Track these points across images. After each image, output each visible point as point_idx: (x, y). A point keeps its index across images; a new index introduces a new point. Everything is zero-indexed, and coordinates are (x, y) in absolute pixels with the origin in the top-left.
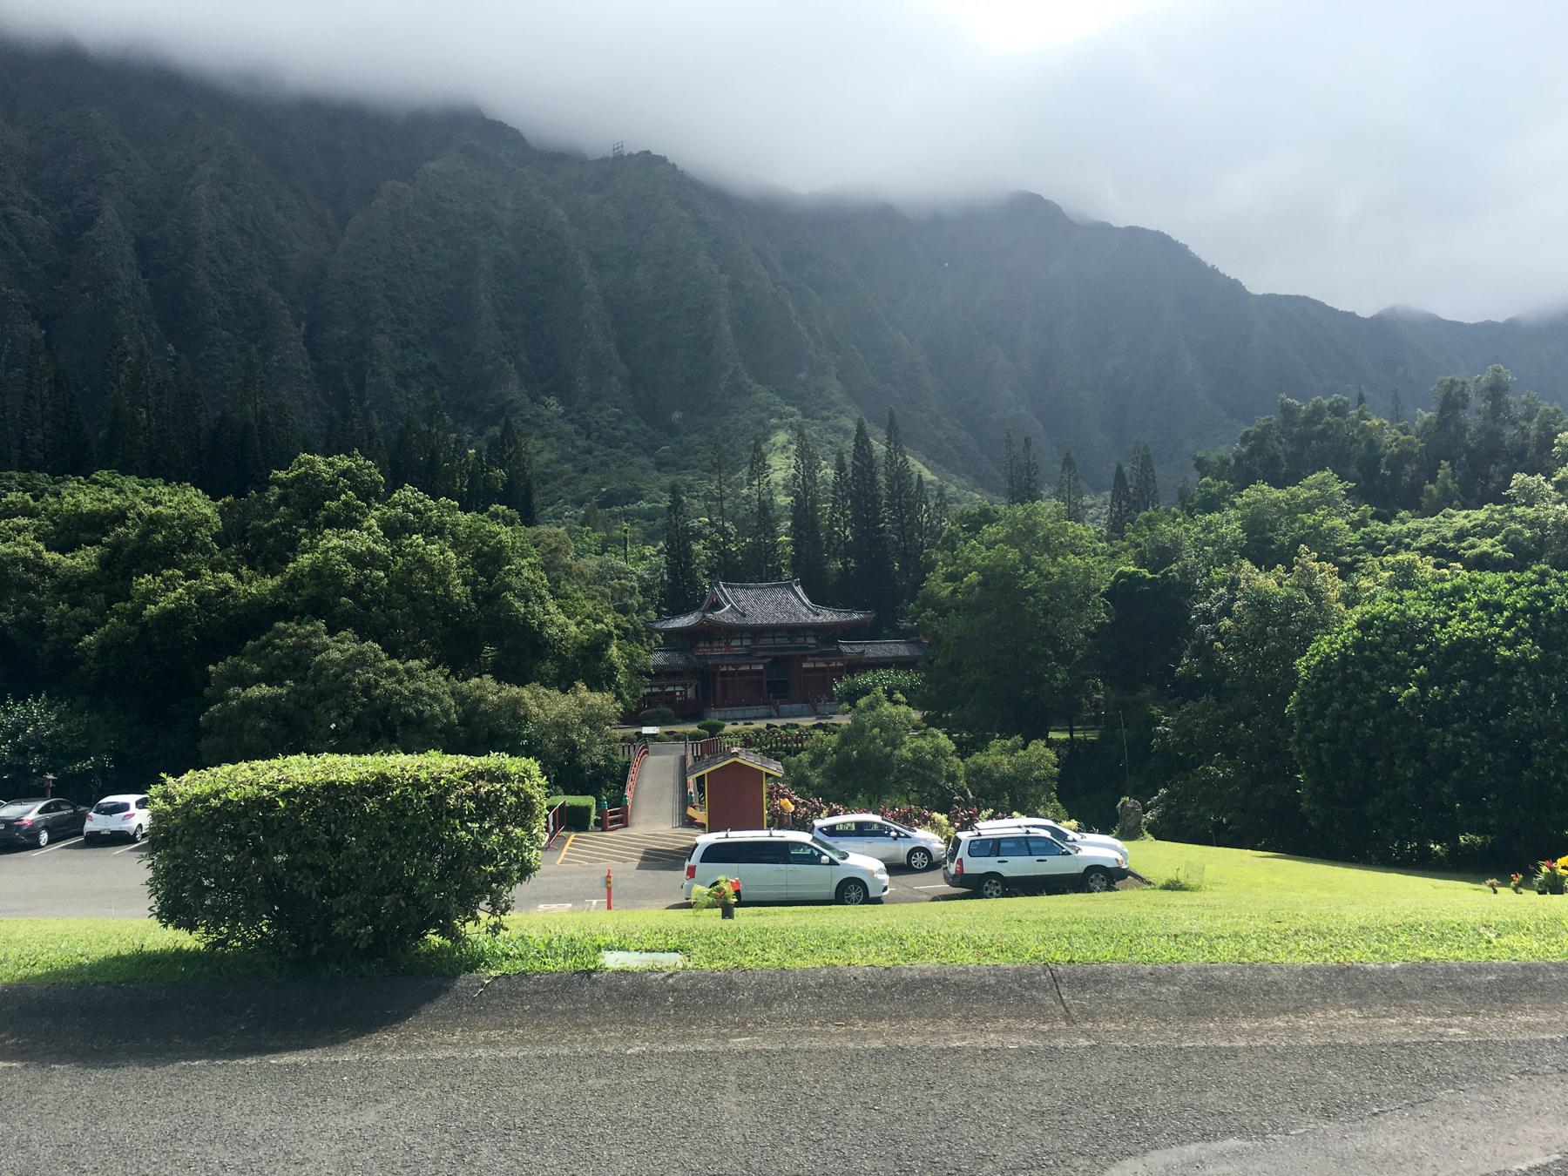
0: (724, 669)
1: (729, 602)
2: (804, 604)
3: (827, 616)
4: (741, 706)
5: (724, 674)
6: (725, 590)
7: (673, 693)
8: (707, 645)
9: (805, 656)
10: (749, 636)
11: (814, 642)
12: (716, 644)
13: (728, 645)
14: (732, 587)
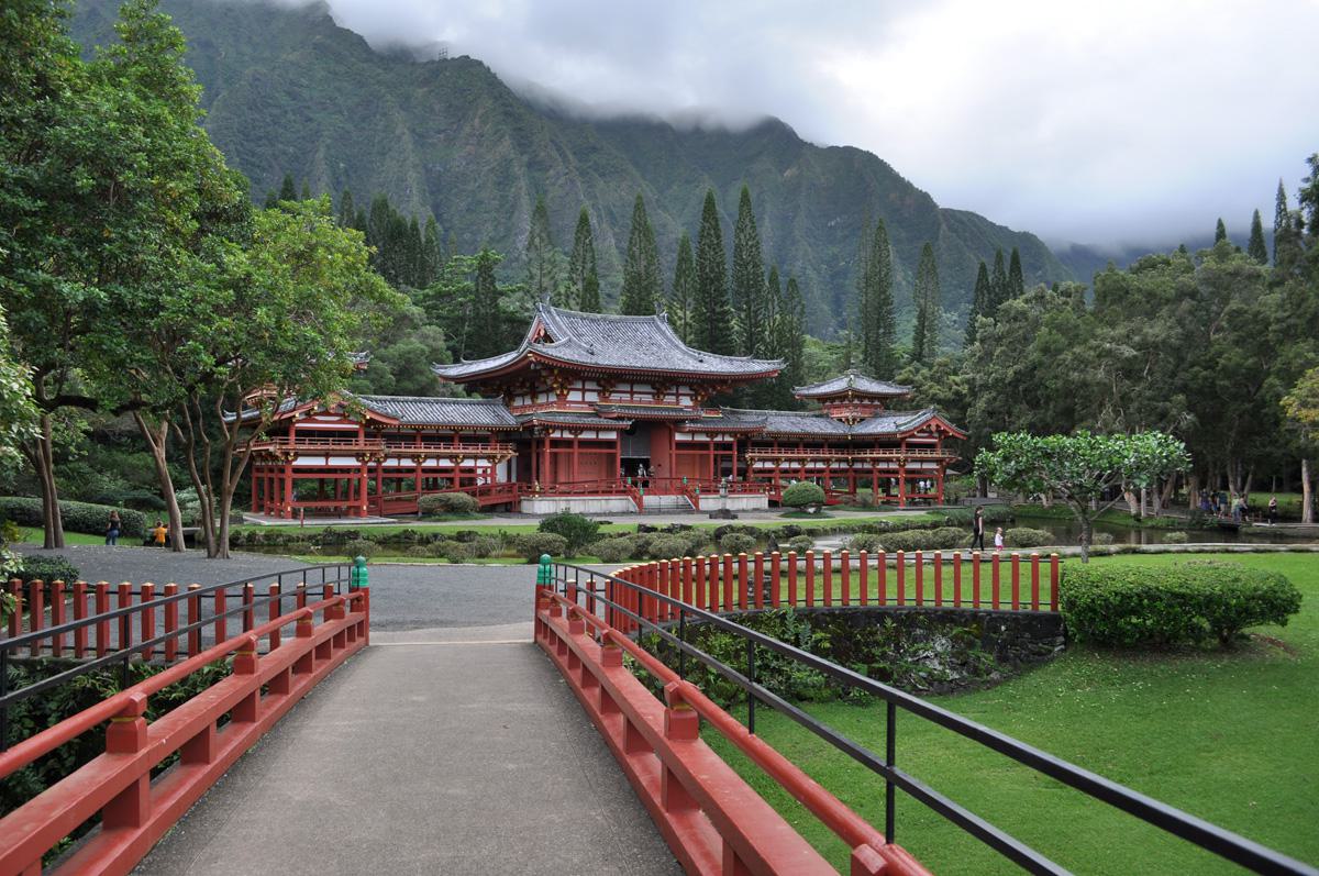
0: (557, 435)
1: (565, 334)
2: (677, 346)
3: (715, 364)
4: (583, 493)
5: (555, 443)
6: (557, 318)
7: (471, 470)
8: (528, 402)
9: (683, 421)
10: (595, 387)
11: (691, 404)
12: (542, 399)
14: (568, 316)
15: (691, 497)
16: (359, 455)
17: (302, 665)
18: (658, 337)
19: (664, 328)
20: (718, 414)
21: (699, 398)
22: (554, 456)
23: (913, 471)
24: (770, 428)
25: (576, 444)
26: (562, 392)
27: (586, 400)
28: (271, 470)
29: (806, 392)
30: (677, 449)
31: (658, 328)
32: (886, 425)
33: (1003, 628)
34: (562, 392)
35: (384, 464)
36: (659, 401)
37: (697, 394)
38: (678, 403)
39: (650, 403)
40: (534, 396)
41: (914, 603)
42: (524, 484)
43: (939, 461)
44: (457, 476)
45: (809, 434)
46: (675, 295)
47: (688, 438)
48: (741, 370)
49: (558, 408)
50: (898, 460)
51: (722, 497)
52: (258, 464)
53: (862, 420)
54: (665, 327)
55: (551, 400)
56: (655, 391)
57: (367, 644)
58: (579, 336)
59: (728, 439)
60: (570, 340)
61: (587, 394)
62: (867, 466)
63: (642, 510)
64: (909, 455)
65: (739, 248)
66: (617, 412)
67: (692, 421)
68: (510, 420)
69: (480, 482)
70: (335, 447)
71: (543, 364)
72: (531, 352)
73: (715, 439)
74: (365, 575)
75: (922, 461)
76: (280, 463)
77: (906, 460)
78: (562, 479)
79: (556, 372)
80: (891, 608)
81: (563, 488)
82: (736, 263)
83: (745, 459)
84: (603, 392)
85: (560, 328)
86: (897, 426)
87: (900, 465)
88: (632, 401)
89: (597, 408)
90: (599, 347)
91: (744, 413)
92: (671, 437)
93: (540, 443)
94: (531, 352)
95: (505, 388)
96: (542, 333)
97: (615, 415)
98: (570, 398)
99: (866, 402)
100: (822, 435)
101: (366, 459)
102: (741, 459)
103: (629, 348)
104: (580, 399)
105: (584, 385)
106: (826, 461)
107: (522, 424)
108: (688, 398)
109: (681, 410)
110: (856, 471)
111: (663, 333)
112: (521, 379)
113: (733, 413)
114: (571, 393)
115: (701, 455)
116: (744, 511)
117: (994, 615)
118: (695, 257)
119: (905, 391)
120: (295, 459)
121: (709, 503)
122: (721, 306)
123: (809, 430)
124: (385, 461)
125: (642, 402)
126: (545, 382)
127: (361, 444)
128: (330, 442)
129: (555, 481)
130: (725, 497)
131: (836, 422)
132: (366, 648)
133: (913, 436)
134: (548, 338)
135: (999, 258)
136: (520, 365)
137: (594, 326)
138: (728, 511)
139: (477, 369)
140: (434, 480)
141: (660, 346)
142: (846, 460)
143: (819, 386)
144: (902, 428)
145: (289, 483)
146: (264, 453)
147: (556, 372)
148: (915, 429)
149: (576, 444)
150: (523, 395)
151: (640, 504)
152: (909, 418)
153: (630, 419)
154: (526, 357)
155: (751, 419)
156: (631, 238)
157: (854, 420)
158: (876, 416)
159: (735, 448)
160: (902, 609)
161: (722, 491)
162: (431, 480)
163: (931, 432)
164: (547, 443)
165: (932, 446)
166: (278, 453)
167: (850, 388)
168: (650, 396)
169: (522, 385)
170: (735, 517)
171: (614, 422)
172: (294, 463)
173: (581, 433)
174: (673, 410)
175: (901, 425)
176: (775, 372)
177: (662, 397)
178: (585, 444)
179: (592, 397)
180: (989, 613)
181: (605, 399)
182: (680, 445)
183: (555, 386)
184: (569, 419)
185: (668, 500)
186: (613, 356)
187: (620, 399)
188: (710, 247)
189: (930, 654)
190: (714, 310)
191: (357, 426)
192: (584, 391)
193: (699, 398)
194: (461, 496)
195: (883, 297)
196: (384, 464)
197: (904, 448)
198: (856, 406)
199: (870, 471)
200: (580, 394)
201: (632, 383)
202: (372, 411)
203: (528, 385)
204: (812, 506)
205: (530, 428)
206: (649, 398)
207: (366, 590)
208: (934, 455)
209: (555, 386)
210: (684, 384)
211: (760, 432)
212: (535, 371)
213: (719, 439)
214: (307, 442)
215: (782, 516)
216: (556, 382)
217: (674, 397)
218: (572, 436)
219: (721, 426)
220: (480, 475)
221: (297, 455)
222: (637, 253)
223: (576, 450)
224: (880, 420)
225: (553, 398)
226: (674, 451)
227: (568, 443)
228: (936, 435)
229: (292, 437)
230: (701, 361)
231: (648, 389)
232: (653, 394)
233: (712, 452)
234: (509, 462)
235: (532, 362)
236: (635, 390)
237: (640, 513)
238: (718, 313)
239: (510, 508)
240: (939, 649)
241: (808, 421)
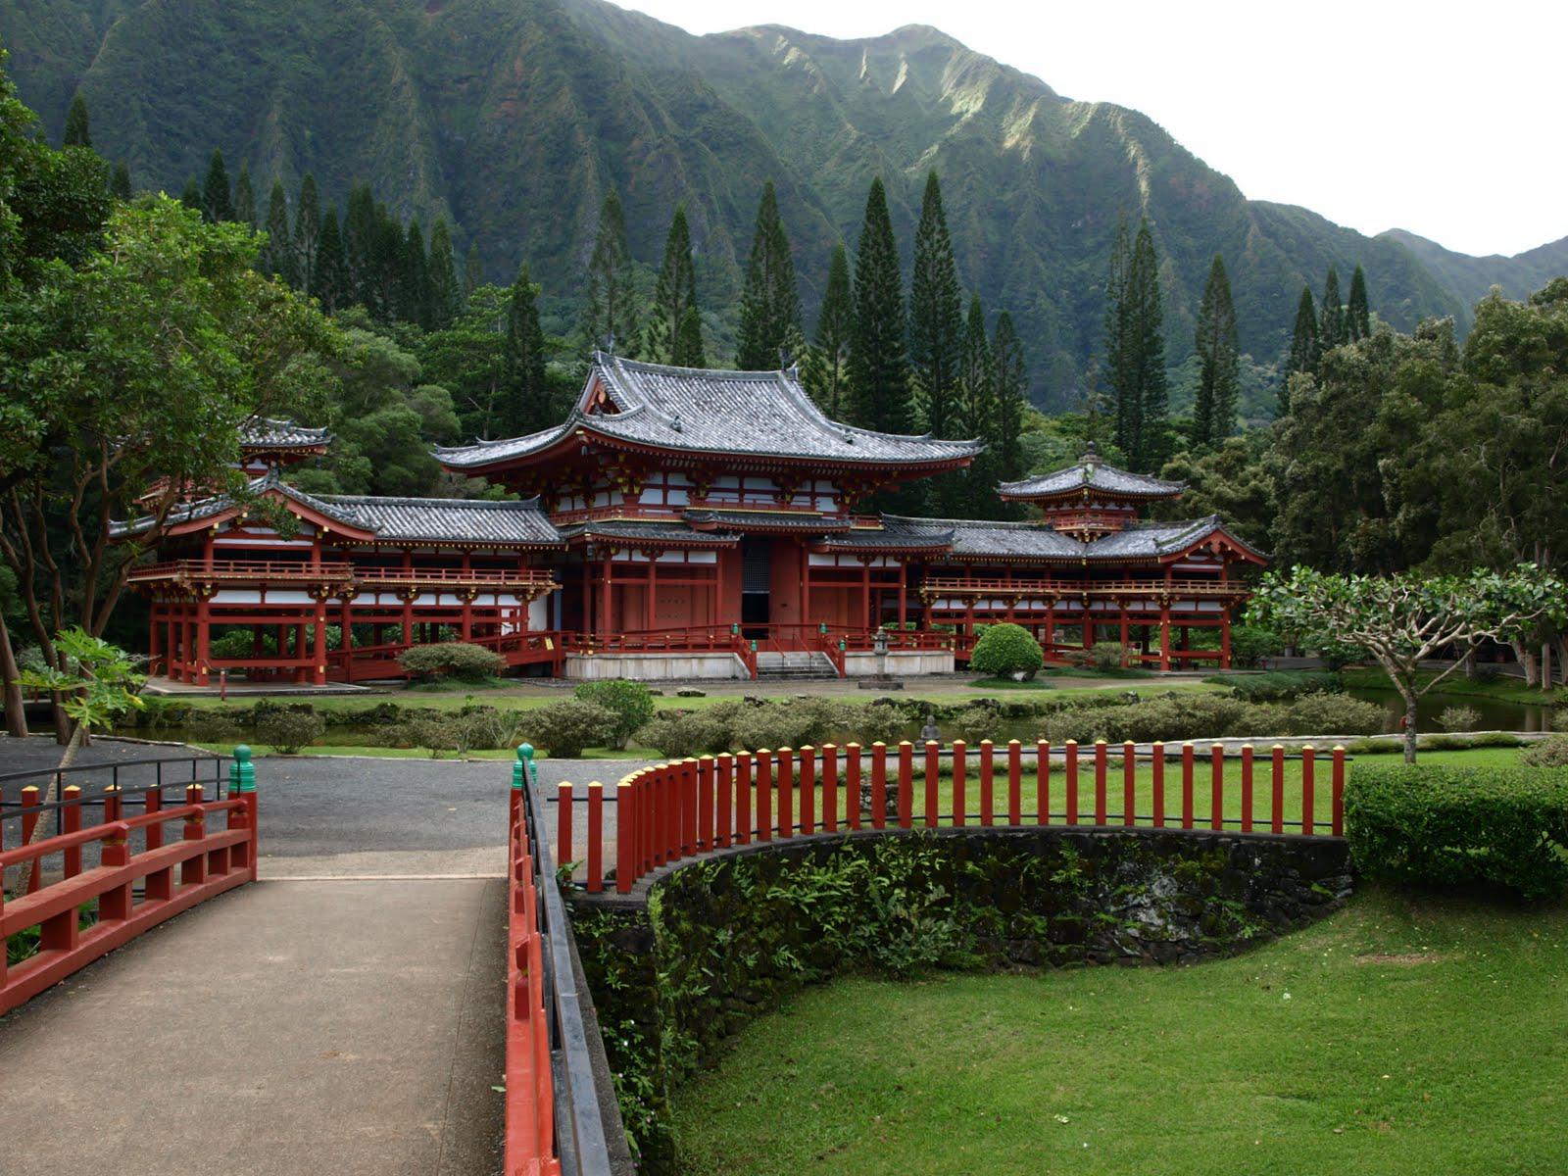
0: (622, 557)
2: (813, 420)
3: (871, 447)
4: (662, 649)
5: (620, 570)
6: (625, 375)
7: (493, 611)
8: (580, 506)
9: (821, 536)
11: (833, 508)
12: (601, 502)
13: (632, 500)
14: (643, 371)
15: (832, 655)
16: (312, 588)
17: (112, 902)
18: (784, 405)
19: (792, 390)
20: (876, 524)
21: (847, 501)
22: (619, 590)
23: (1184, 616)
24: (961, 547)
25: (653, 573)
26: (631, 490)
27: (670, 502)
28: (178, 611)
29: (1016, 491)
30: (811, 580)
31: (783, 389)
32: (1139, 543)
33: (1257, 861)
34: (631, 490)
35: (353, 602)
36: (785, 505)
38: (813, 507)
39: (769, 507)
40: (589, 497)
41: (1121, 822)
42: (572, 634)
43: (1223, 600)
44: (470, 621)
45: (1020, 557)
46: (823, 337)
47: (830, 563)
48: (912, 456)
49: (626, 515)
50: (1159, 597)
51: (878, 655)
52: (159, 600)
53: (1105, 534)
54: (795, 389)
55: (613, 503)
56: (778, 489)
57: (253, 879)
58: (660, 402)
59: (892, 564)
60: (644, 409)
62: (1112, 607)
63: (759, 675)
64: (1177, 590)
65: (922, 263)
66: (716, 521)
67: (835, 535)
68: (549, 533)
69: (506, 630)
70: (275, 576)
71: (601, 446)
72: (580, 428)
73: (872, 565)
74: (250, 773)
75: (1197, 599)
76: (191, 600)
77: (1171, 598)
78: (632, 624)
79: (621, 458)
80: (1084, 829)
81: (634, 641)
82: (917, 288)
83: (920, 595)
84: (695, 492)
85: (629, 390)
86: (1158, 545)
87: (1161, 605)
89: (686, 515)
90: (690, 419)
91: (919, 524)
92: (803, 560)
93: (597, 569)
94: (580, 428)
95: (544, 484)
96: (602, 399)
97: (715, 527)
98: (643, 500)
99: (1112, 507)
100: (1041, 558)
101: (324, 595)
102: (913, 595)
103: (737, 421)
104: (660, 501)
105: (665, 480)
106: (1047, 599)
107: (568, 539)
109: (818, 518)
110: (1094, 614)
111: (792, 399)
112: (568, 470)
113: (903, 523)
114: (646, 492)
115: (850, 590)
116: (911, 676)
117: (1243, 842)
118: (853, 277)
119: (1173, 489)
120: (213, 594)
121: (859, 664)
122: (893, 356)
123: (1020, 550)
124: (355, 597)
125: (759, 509)
126: (605, 475)
127: (316, 572)
128: (268, 568)
129: (620, 625)
130: (884, 655)
131: (1063, 539)
132: (251, 882)
133: (1183, 560)
134: (610, 407)
135: (1332, 281)
136: (565, 449)
137: (683, 387)
138: (887, 677)
139: (501, 454)
140: (434, 625)
141: (785, 419)
142: (1079, 598)
143: (1038, 481)
144: (1166, 548)
145: (203, 632)
146: (166, 585)
147: (621, 458)
148: (1186, 549)
149: (653, 573)
150: (572, 495)
151: (750, 661)
152: (1179, 531)
153: (736, 532)
154: (574, 436)
155: (930, 530)
156: (756, 248)
157: (1092, 534)
158: (1128, 529)
159: (903, 578)
160: (1100, 831)
161: (879, 648)
162: (428, 626)
163: (1211, 554)
164: (608, 570)
165: (1213, 576)
166: (187, 585)
167: (1085, 484)
168: (771, 497)
169: (571, 480)
170: (899, 686)
171: (711, 538)
172: (212, 600)
173: (661, 555)
174: (809, 518)
175: (1164, 543)
176: (965, 458)
177: (788, 498)
179: (678, 498)
180: (1235, 838)
181: (699, 500)
182: (818, 573)
183: (620, 480)
184: (642, 533)
185: (795, 659)
186: (710, 434)
187: (721, 505)
188: (876, 262)
189: (1146, 900)
190: (882, 360)
191: (310, 544)
192: (666, 488)
193: (847, 501)
194: (477, 652)
195: (1146, 340)
196: (353, 602)
197: (1168, 581)
198: (1095, 513)
199: (1115, 615)
200: (660, 493)
201: (742, 476)
202: (332, 519)
203: (579, 478)
204: (1019, 670)
205: (578, 545)
206: (768, 500)
207: (252, 797)
208: (1216, 591)
209: (620, 480)
210: (823, 478)
211: (942, 549)
212: (589, 456)
213: (877, 564)
214: (232, 567)
215: (972, 685)
216: (621, 474)
217: (808, 499)
218: (647, 560)
219: (879, 543)
220: (506, 620)
221: (217, 588)
222: (763, 270)
223: (653, 581)
224: (1133, 535)
225: (617, 500)
226: (807, 584)
227: (641, 570)
228: (1220, 559)
229: (209, 561)
230: (850, 442)
231: (767, 485)
232: (775, 494)
233: (867, 585)
234: (550, 599)
235: (582, 443)
236: (746, 486)
237: (753, 678)
238: (888, 367)
239: (548, 670)
240: (1158, 892)
241: (1020, 536)
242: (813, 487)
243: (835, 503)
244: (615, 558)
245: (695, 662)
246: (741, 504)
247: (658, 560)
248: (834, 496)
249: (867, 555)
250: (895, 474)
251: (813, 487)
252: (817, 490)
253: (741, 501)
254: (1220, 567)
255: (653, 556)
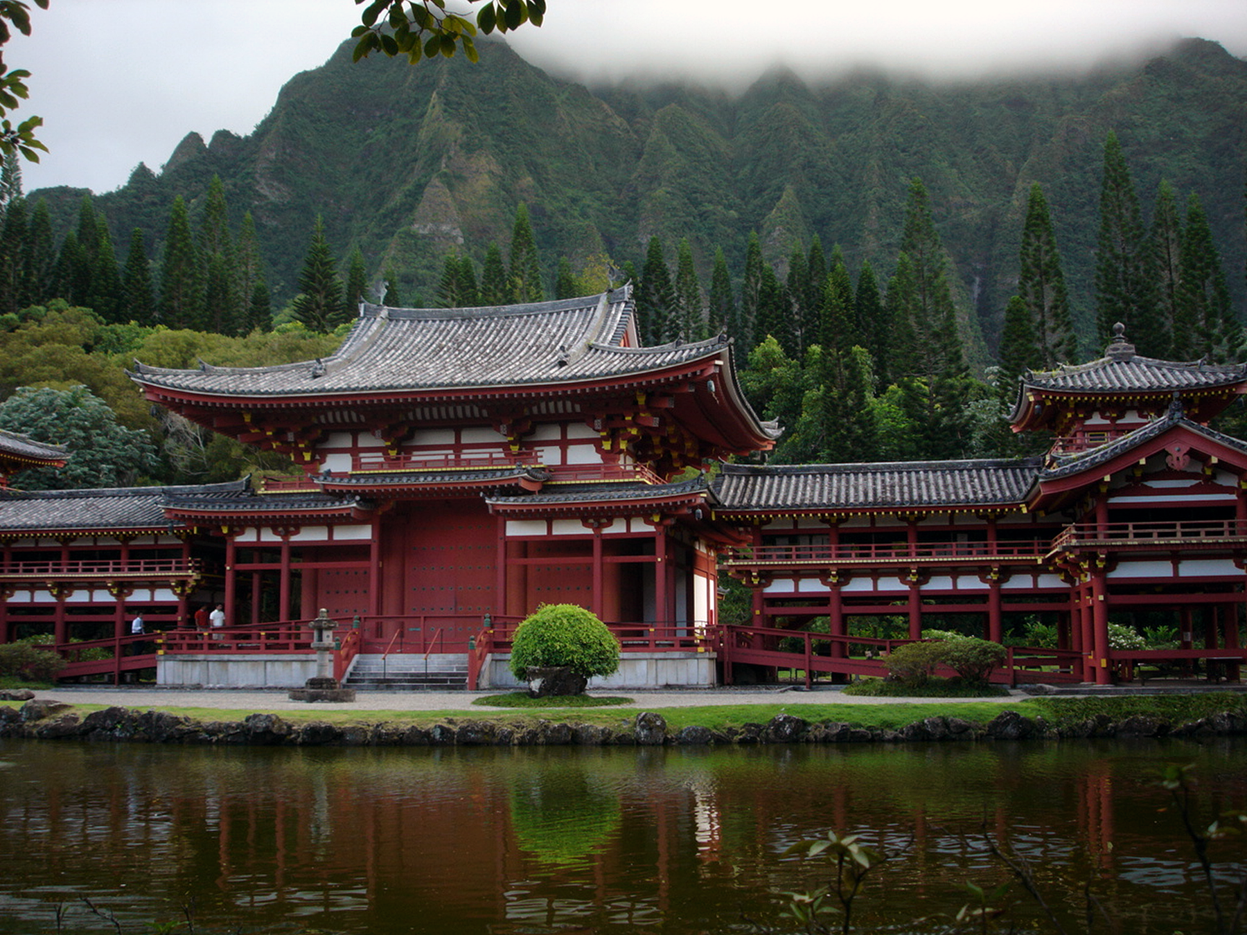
0: (249, 537)
11: (596, 459)
37: (614, 436)
47: (537, 530)
59: (640, 527)
61: (366, 458)
73: (606, 531)
79: (247, 419)
88: (458, 461)
105: (355, 442)
108: (592, 447)
147: (247, 419)
159: (660, 545)
164: (230, 553)
173: (297, 532)
178: (302, 551)
192: (355, 451)
201: (457, 426)
206: (498, 454)
213: (618, 528)
218: (278, 539)
227: (271, 551)
242: (564, 433)
243: (599, 449)
244: (239, 539)
245: (296, 666)
246: (458, 461)
247: (294, 538)
248: (597, 443)
249: (597, 515)
250: (641, 400)
251: (564, 433)
252: (569, 437)
253: (458, 456)
254: (1234, 497)
255: (287, 534)
